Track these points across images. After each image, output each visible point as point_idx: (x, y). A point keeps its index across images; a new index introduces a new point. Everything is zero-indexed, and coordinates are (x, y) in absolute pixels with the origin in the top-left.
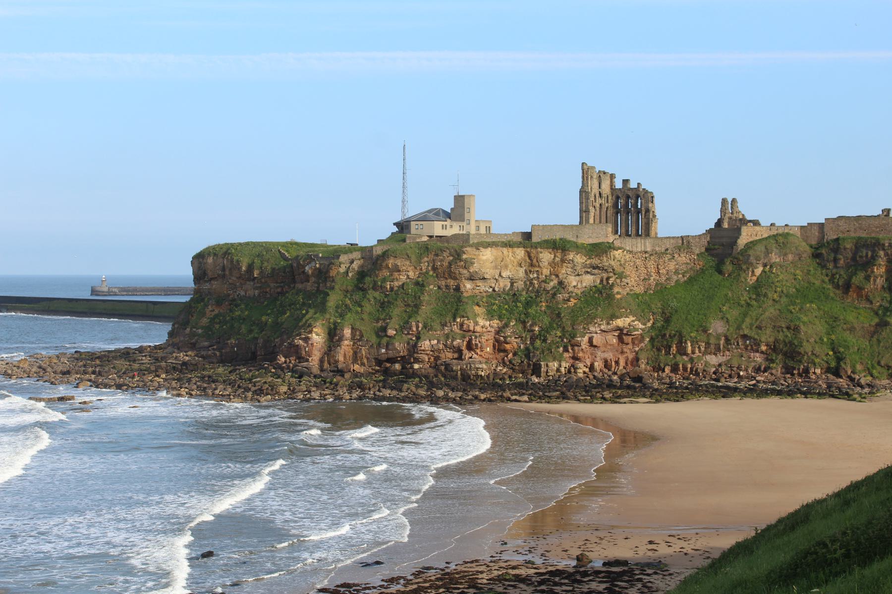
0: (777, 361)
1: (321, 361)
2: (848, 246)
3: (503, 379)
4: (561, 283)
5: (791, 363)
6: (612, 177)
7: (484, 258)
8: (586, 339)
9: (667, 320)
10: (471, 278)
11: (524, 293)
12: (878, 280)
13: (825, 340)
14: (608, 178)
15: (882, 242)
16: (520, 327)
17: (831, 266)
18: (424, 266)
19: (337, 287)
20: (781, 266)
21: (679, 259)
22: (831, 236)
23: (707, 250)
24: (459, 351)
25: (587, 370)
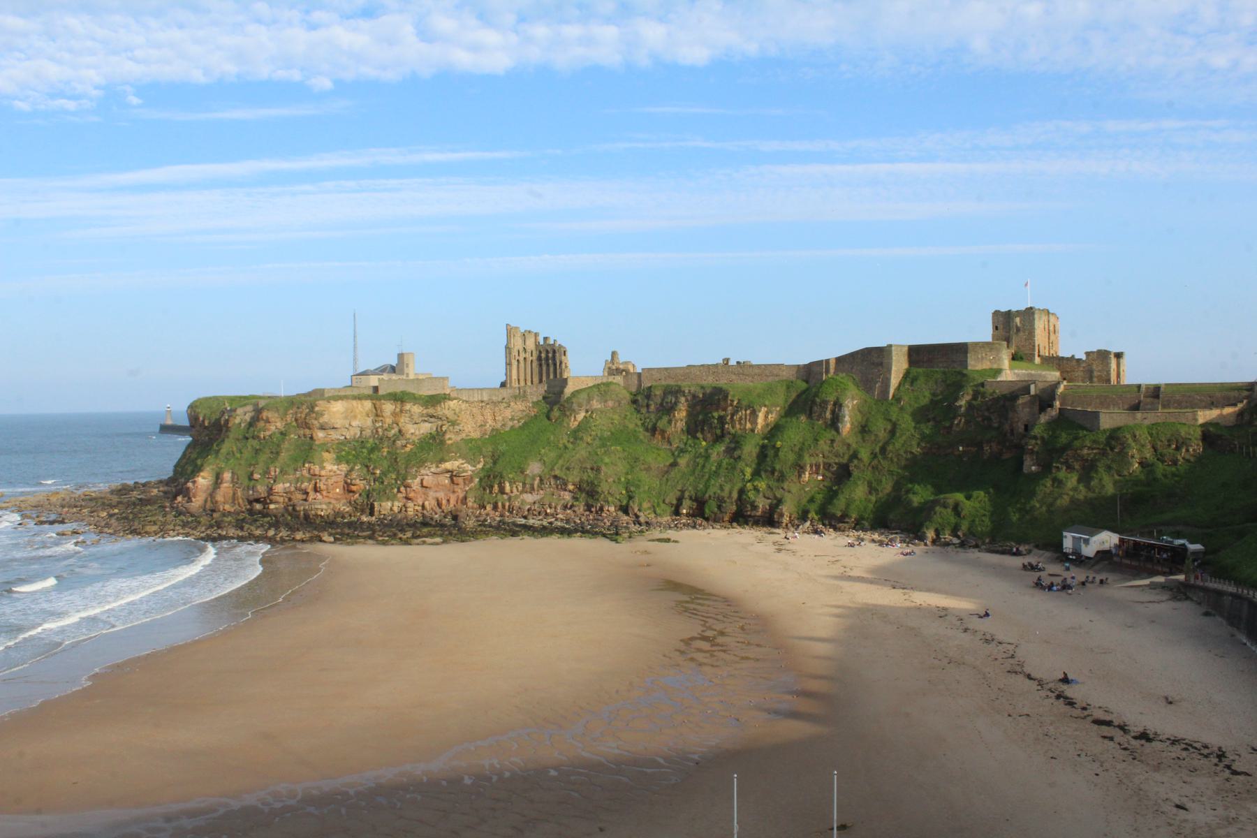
1: (206, 501)
3: (343, 517)
4: (400, 431)
5: (591, 501)
6: (536, 335)
8: (418, 480)
9: (495, 463)
10: (322, 428)
16: (365, 470)
17: (644, 410)
18: (289, 417)
19: (231, 435)
22: (646, 384)
23: (544, 398)
24: (307, 493)
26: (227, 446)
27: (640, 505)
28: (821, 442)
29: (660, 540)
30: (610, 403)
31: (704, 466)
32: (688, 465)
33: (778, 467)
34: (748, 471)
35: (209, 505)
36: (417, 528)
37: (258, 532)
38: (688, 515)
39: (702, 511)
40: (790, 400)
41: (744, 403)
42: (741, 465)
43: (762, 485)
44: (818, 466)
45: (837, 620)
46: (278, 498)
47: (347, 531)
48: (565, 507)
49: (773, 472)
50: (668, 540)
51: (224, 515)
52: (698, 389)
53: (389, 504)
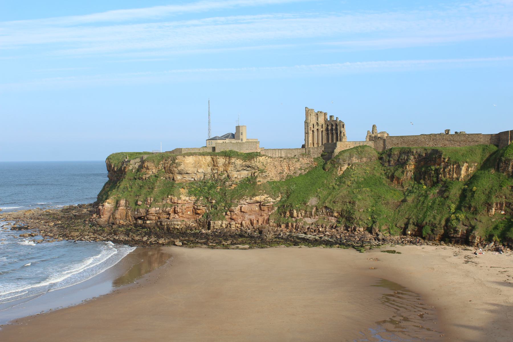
0: (342, 223)
1: (110, 218)
2: (396, 153)
4: (228, 176)
6: (325, 114)
7: (188, 162)
8: (239, 207)
9: (288, 197)
10: (180, 173)
11: (210, 181)
12: (408, 174)
13: (370, 210)
14: (323, 114)
15: (412, 150)
17: (386, 164)
18: (160, 166)
19: (127, 177)
20: (358, 165)
21: (303, 161)
23: (322, 155)
25: (240, 225)
26: (124, 183)
27: (380, 227)
28: (504, 188)
29: (388, 252)
30: (364, 160)
31: (423, 202)
32: (413, 202)
33: (473, 204)
34: (453, 207)
35: (111, 220)
36: (235, 238)
37: (137, 238)
38: (411, 235)
39: (420, 233)
40: (485, 159)
41: (452, 160)
42: (448, 202)
43: (462, 216)
44: (501, 204)
45: (490, 314)
46: (151, 217)
47: (192, 239)
48: (332, 227)
49: (470, 208)
50: (394, 252)
51: (119, 227)
52: (422, 150)
53: (220, 222)
